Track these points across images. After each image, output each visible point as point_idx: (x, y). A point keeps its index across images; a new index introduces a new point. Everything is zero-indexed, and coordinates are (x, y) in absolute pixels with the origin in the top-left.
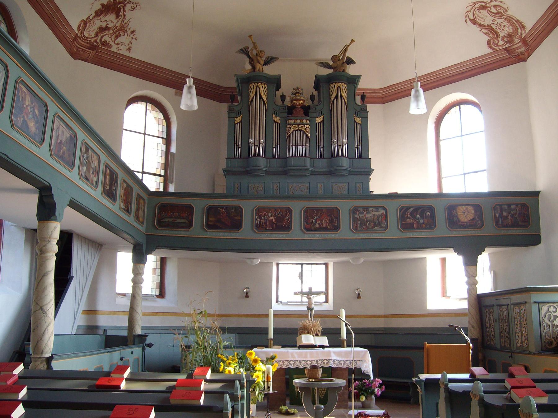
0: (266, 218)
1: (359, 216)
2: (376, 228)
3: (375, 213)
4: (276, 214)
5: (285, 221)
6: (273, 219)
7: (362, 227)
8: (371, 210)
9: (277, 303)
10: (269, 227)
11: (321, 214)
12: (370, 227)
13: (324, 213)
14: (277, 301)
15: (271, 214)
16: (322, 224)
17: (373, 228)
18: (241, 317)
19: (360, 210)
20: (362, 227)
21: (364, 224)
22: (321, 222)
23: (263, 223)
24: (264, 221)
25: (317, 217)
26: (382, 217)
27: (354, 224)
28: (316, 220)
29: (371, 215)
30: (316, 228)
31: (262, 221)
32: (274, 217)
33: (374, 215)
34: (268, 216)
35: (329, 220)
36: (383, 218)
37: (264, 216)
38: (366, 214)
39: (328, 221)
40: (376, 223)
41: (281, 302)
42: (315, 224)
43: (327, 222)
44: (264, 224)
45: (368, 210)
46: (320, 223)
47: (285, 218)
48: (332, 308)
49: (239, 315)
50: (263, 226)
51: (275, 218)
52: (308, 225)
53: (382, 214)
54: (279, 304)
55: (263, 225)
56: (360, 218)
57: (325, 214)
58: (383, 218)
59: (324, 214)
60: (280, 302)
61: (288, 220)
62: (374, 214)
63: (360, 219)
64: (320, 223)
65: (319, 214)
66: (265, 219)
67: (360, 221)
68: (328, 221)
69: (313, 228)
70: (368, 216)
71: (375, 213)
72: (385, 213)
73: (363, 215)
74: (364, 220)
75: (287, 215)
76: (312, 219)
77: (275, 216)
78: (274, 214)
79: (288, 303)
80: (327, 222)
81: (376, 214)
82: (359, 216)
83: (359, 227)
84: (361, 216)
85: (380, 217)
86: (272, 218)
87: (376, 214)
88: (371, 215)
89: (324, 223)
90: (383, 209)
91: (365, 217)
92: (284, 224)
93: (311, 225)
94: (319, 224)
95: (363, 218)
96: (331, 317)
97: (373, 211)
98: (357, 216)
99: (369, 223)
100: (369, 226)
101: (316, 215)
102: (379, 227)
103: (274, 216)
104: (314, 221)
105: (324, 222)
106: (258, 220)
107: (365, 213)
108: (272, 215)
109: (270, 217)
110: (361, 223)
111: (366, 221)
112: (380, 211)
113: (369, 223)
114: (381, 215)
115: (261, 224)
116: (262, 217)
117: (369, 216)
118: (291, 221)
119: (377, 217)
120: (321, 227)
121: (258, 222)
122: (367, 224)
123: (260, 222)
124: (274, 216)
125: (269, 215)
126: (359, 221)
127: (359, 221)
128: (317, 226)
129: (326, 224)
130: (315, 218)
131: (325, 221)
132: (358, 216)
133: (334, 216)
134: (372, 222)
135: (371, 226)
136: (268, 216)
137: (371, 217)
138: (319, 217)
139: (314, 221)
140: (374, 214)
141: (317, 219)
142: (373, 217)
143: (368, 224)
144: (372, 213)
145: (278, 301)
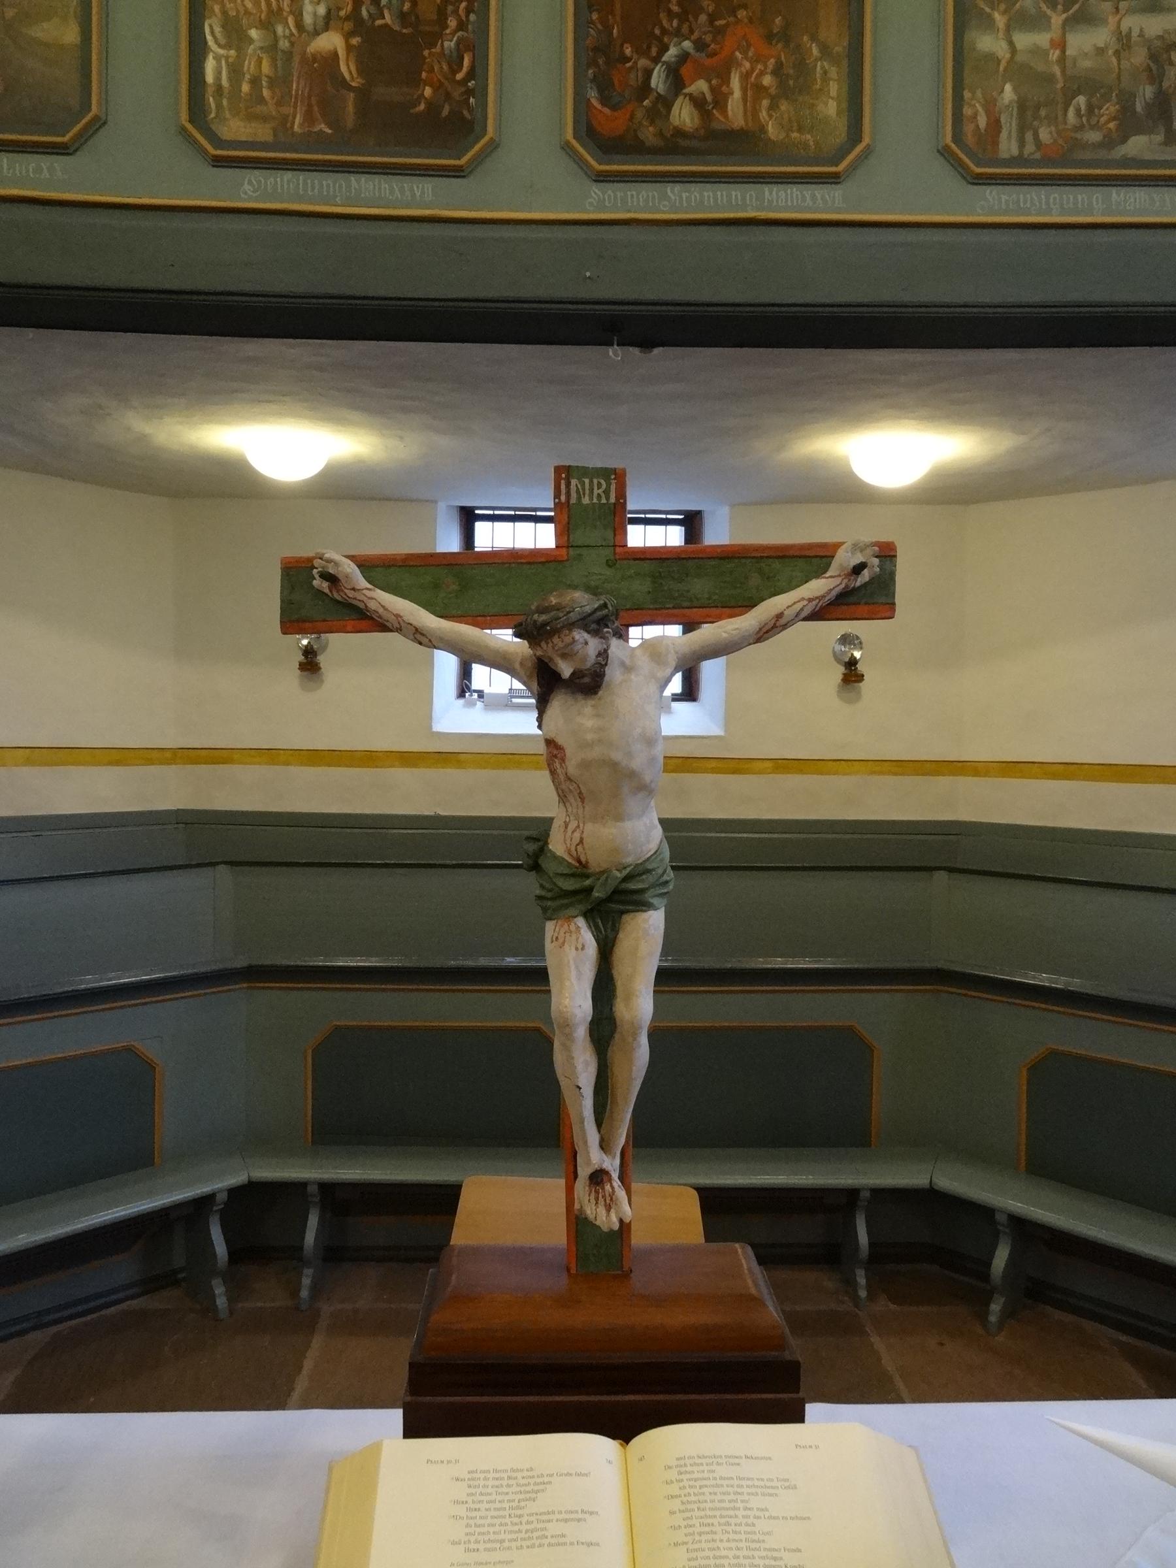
0: (284, 44)
1: (1011, 43)
2: (1137, 145)
3: (1133, 23)
4: (364, 13)
5: (431, 70)
6: (335, 55)
7: (1029, 136)
9: (461, 701)
10: (309, 118)
11: (712, 19)
12: (1094, 137)
13: (742, 14)
14: (464, 689)
15: (322, 10)
16: (720, 99)
17: (1109, 143)
18: (287, 764)
20: (1029, 136)
22: (712, 89)
23: (255, 82)
24: (266, 68)
25: (687, 45)
28: (677, 81)
29: (1101, 36)
30: (679, 133)
31: (249, 66)
32: (347, 36)
33: (1124, 42)
34: (300, 25)
35: (777, 71)
37: (266, 25)
39: (767, 80)
40: (1139, 108)
41: (481, 694)
42: (666, 103)
43: (759, 89)
44: (266, 93)
46: (709, 98)
47: (438, 49)
48: (714, 729)
49: (271, 755)
50: (259, 109)
51: (355, 41)
52: (614, 108)
54: (472, 704)
55: (261, 100)
56: (1019, 58)
57: (751, 20)
59: (738, 21)
60: (475, 695)
61: (462, 58)
63: (1019, 71)
64: (709, 98)
65: (703, 18)
66: (272, 48)
68: (767, 80)
69: (649, 134)
70: (1082, 42)
71: (1133, 23)
73: (1042, 39)
74: (1050, 79)
75: (452, 23)
76: (643, 62)
77: (356, 26)
78: (342, 13)
79: (514, 700)
80: (766, 89)
81: (1141, 35)
82: (1011, 43)
83: (1004, 135)
84: (1023, 40)
86: (331, 41)
87: (1141, 35)
88: (1101, 36)
89: (737, 94)
91: (1055, 55)
92: (428, 91)
93: (639, 114)
94: (698, 102)
95: (1040, 67)
96: (714, 771)
98: (988, 43)
101: (678, 33)
102: (1159, 138)
103: (348, 26)
104: (658, 80)
105: (735, 83)
106: (217, 58)
107: (1057, 20)
108: (328, 17)
109: (317, 33)
110: (1022, 105)
113: (1081, 100)
115: (245, 88)
116: (254, 33)
118: (477, 72)
119: (1153, 57)
120: (715, 125)
121: (218, 73)
123: (236, 71)
124: (348, 26)
125: (308, 19)
126: (1008, 88)
127: (1008, 88)
128: (683, 115)
129: (752, 112)
130: (672, 53)
131: (745, 77)
132: (1004, 45)
133: (814, 38)
134: (1106, 98)
135: (1095, 127)
136: (300, 25)
137: (1100, 51)
138: (700, 45)
139: (658, 80)
140: (1124, 26)
141: (684, 57)
142: (1117, 53)
143: (1078, 110)
144: (1112, 20)
145: (469, 688)
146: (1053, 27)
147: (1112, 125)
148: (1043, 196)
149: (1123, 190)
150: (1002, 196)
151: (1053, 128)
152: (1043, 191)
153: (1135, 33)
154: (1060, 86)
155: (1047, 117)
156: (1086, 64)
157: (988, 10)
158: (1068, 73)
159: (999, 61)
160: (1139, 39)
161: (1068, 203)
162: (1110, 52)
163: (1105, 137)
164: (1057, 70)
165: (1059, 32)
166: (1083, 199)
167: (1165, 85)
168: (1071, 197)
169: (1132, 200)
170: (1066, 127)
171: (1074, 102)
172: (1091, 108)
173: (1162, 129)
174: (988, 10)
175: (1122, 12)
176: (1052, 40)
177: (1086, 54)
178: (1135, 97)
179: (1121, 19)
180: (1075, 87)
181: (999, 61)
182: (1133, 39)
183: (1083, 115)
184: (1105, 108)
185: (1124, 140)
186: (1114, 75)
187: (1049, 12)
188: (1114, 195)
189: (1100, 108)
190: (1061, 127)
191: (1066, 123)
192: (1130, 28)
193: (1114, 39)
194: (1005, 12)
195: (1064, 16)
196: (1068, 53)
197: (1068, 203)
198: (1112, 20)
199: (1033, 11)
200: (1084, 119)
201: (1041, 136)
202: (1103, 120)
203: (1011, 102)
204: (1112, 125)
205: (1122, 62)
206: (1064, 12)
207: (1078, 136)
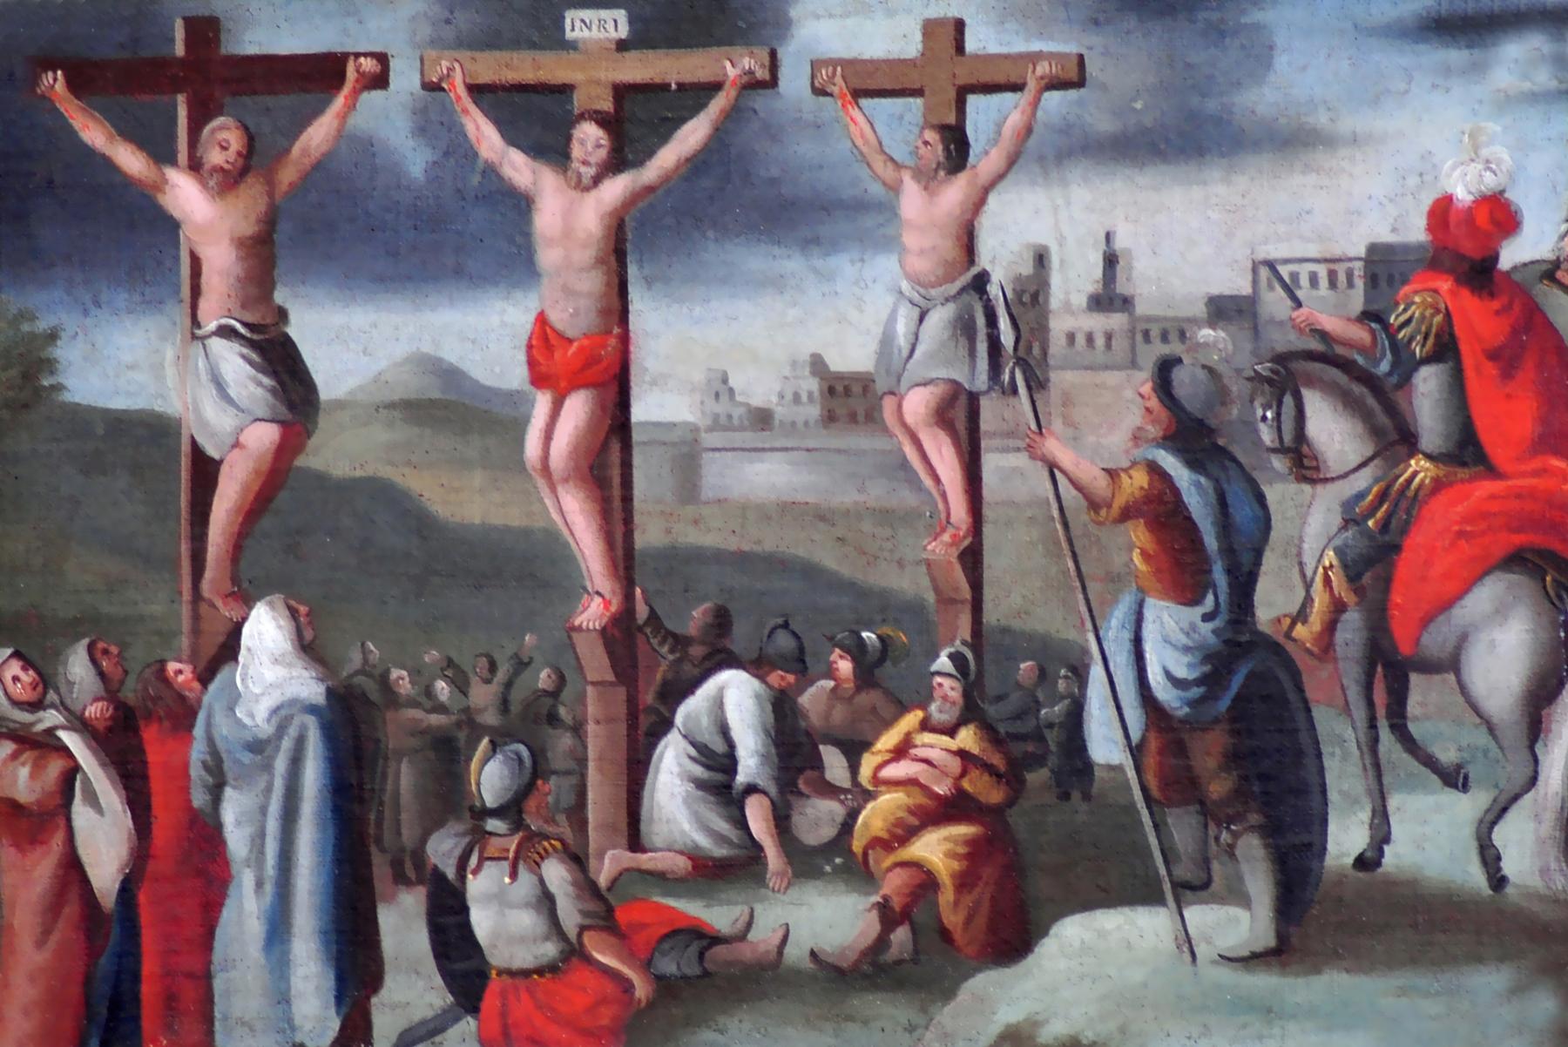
45: (736, 64)
67: (309, 648)
87: (1108, 299)
97: (982, 113)
132: (233, 361)
146: (548, 257)
151: (556, 873)
154: (592, 614)
155: (512, 810)
157: (131, 160)
158: (649, 535)
160: (1098, 323)
162: (917, 404)
163: (889, 916)
165: (592, 283)
170: (645, 860)
171: (693, 708)
174: (131, 160)
175: (985, 158)
176: (544, 338)
177: (762, 419)
178: (1080, 674)
179: (979, 203)
180: (696, 618)
181: (205, 471)
182: (1059, 325)
183: (751, 789)
184: (888, 740)
186: (941, 549)
187: (518, 167)
189: (854, 750)
190: (609, 864)
191: (635, 843)
192: (1041, 259)
193: (939, 318)
194: (228, 182)
195: (616, 188)
196: (642, 410)
199: (415, 160)
200: (757, 815)
201: (482, 921)
202: (876, 815)
203: (283, 715)
205: (993, 463)
206: (617, 163)
207: (719, 916)
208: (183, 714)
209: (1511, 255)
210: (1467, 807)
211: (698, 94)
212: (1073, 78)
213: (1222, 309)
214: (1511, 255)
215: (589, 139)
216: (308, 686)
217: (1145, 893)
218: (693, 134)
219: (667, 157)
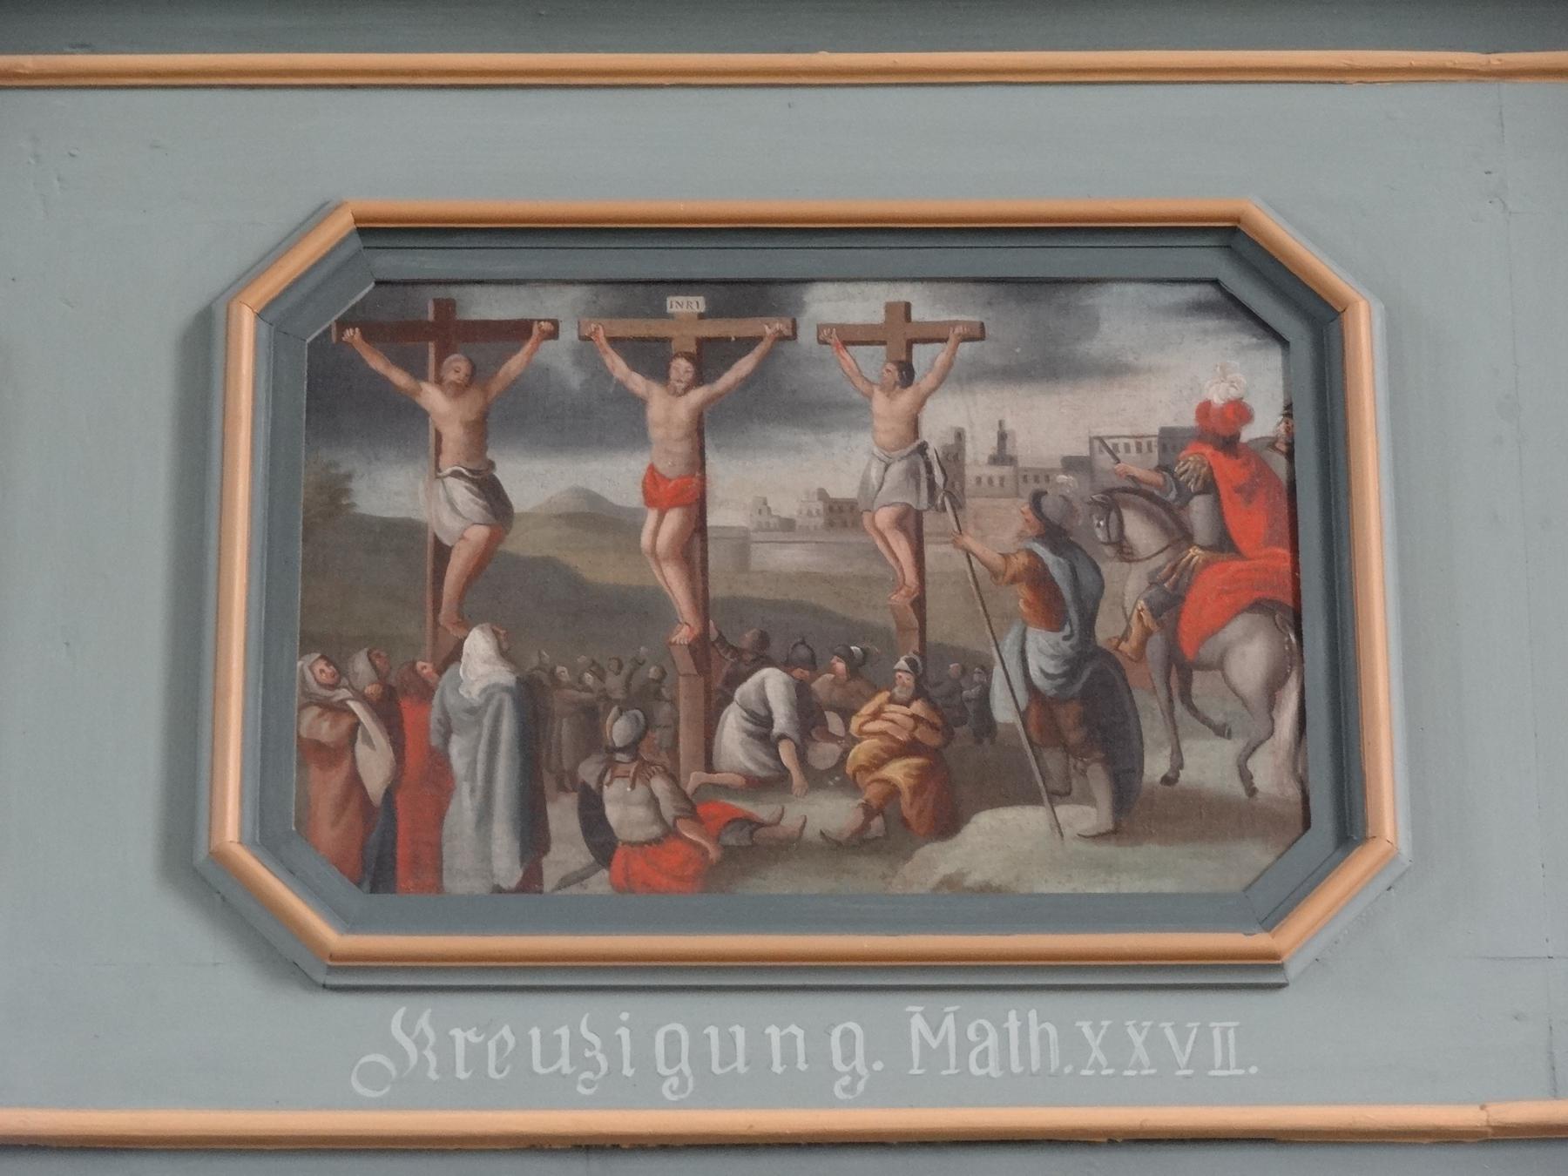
7: (563, 815)
8: (851, 337)
19: (519, 331)
20: (563, 815)
21: (619, 730)
26: (1180, 535)
27: (327, 731)
36: (1224, 543)
38: (699, 429)
40: (1004, 711)
45: (770, 327)
53: (1190, 462)
56: (519, 543)
58: (1224, 543)
62: (954, 456)
67: (505, 654)
72: (1265, 424)
83: (463, 806)
85: (1140, 531)
87: (1001, 457)
90: (1234, 308)
99: (773, 684)
100: (756, 786)
111: (701, 648)
112: (1113, 370)
113: (773, 684)
114: (1141, 467)
117: (786, 506)
122: (732, 727)
126: (478, 644)
127: (478, 644)
132: (461, 492)
135: (839, 778)
140: (935, 431)
142: (912, 525)
143: (761, 723)
144: (888, 409)
146: (656, 433)
147: (897, 771)
148: (624, 1032)
149: (951, 1007)
150: (457, 1033)
151: (659, 785)
152: (625, 1012)
153: (979, 448)
154: (683, 635)
155: (632, 748)
156: (790, 557)
157: (399, 378)
158: (718, 590)
159: (442, 553)
160: (996, 471)
161: (728, 1057)
162: (884, 517)
163: (869, 811)
164: (673, 581)
165: (682, 448)
166: (788, 1041)
167: (1106, 630)
168: (739, 1032)
169: (992, 1041)
170: (715, 778)
171: (747, 689)
172: (808, 713)
173: (1099, 782)
174: (399, 378)
175: (924, 380)
176: (653, 479)
177: (788, 525)
178: (987, 671)
179: (921, 404)
180: (748, 639)
181: (442, 553)
182: (971, 473)
183: (782, 737)
184: (868, 709)
185: (947, 824)
186: (900, 599)
187: (637, 383)
188: (918, 1024)
189: (847, 714)
190: (694, 779)
191: (709, 767)
192: (960, 435)
193: (898, 468)
194: (458, 391)
195: (698, 395)
196: (714, 519)
197: (728, 1057)
198: (888, 409)
199: (575, 379)
200: (786, 752)
201: (613, 813)
202: (861, 752)
203: (489, 692)
204: (897, 771)
205: (930, 551)
206: (699, 380)
207: (762, 810)
208: (426, 692)
209: (1248, 434)
210: (1227, 750)
211: (748, 344)
212: (977, 334)
213: (1072, 464)
214: (1248, 434)
215: (681, 368)
216: (504, 676)
217: (1032, 798)
218: (745, 365)
219: (729, 378)
